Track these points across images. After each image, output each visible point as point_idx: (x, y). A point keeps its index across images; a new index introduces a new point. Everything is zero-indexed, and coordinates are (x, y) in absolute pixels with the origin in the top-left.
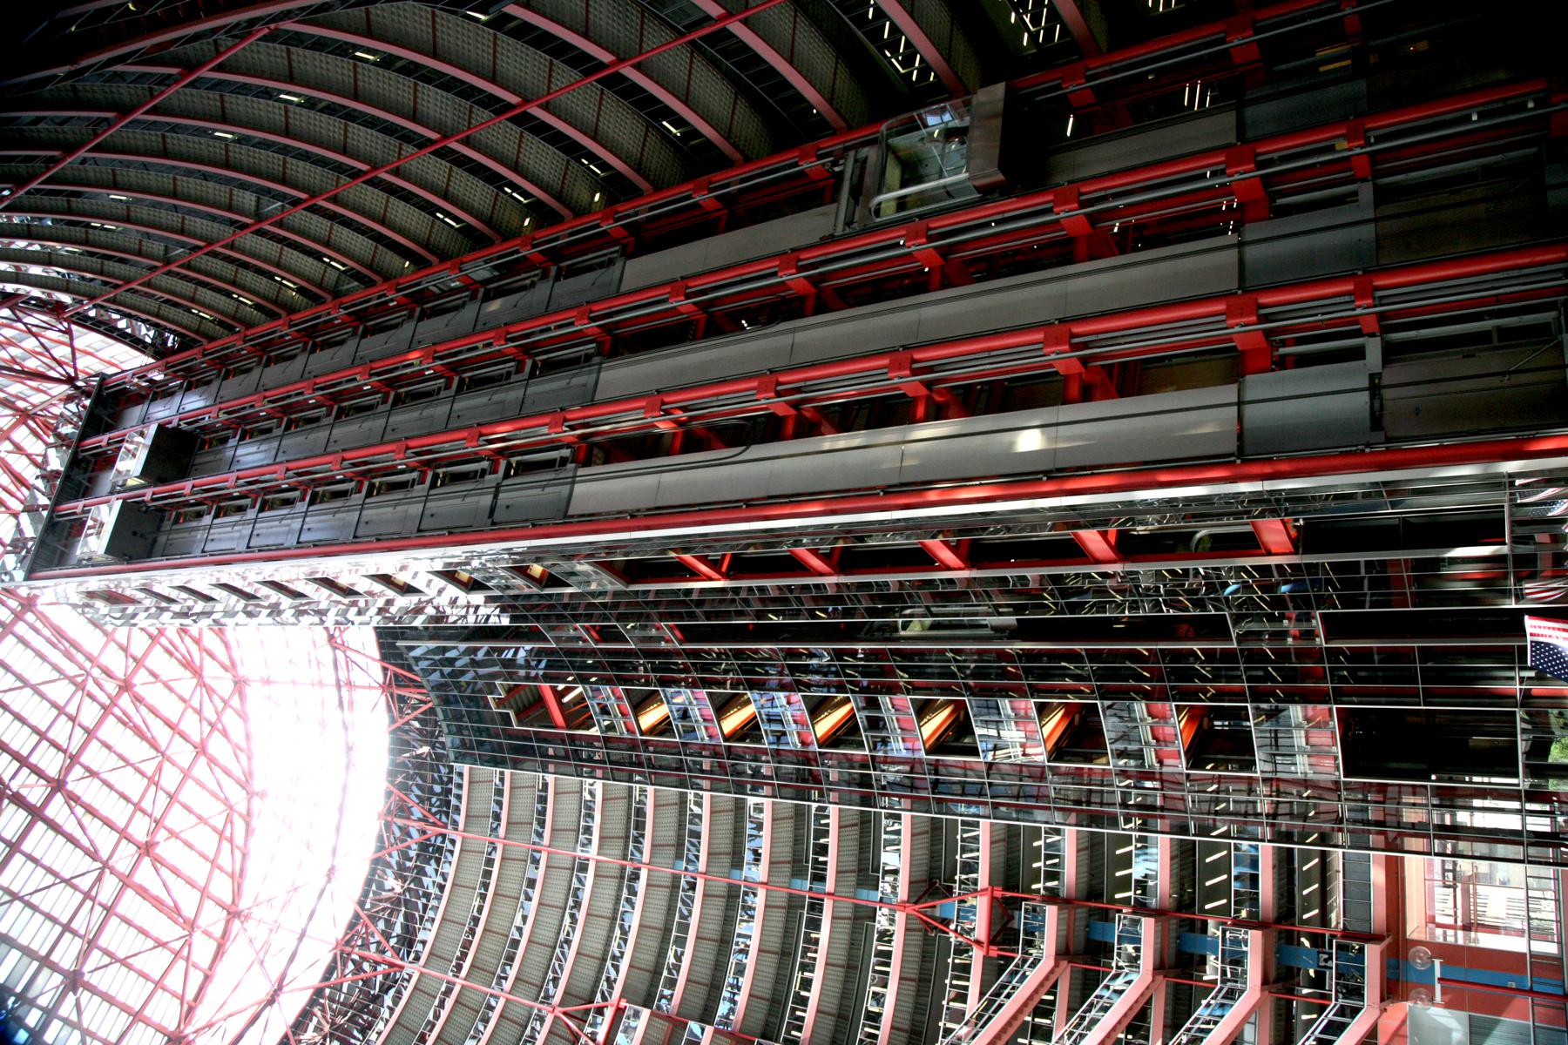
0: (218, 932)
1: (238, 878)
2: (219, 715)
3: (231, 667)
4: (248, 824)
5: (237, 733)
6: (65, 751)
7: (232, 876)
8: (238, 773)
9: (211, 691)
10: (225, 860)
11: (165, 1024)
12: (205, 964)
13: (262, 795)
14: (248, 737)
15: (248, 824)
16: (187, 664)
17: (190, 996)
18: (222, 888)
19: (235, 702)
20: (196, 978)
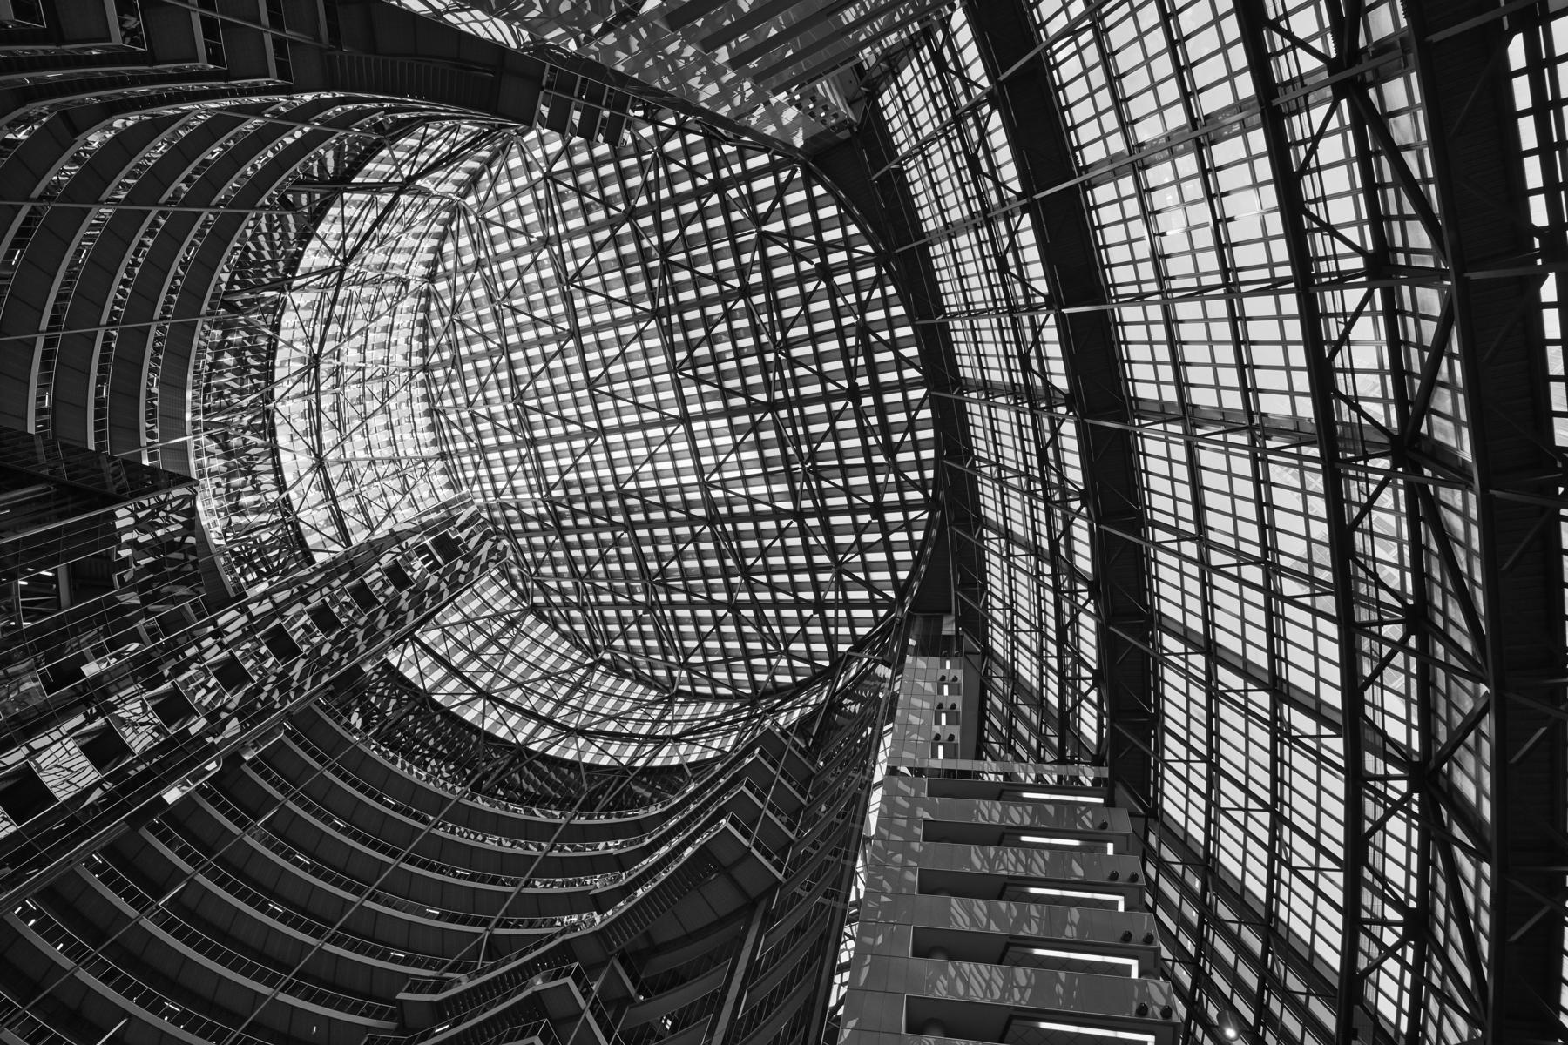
8: (462, 224)
9: (453, 289)
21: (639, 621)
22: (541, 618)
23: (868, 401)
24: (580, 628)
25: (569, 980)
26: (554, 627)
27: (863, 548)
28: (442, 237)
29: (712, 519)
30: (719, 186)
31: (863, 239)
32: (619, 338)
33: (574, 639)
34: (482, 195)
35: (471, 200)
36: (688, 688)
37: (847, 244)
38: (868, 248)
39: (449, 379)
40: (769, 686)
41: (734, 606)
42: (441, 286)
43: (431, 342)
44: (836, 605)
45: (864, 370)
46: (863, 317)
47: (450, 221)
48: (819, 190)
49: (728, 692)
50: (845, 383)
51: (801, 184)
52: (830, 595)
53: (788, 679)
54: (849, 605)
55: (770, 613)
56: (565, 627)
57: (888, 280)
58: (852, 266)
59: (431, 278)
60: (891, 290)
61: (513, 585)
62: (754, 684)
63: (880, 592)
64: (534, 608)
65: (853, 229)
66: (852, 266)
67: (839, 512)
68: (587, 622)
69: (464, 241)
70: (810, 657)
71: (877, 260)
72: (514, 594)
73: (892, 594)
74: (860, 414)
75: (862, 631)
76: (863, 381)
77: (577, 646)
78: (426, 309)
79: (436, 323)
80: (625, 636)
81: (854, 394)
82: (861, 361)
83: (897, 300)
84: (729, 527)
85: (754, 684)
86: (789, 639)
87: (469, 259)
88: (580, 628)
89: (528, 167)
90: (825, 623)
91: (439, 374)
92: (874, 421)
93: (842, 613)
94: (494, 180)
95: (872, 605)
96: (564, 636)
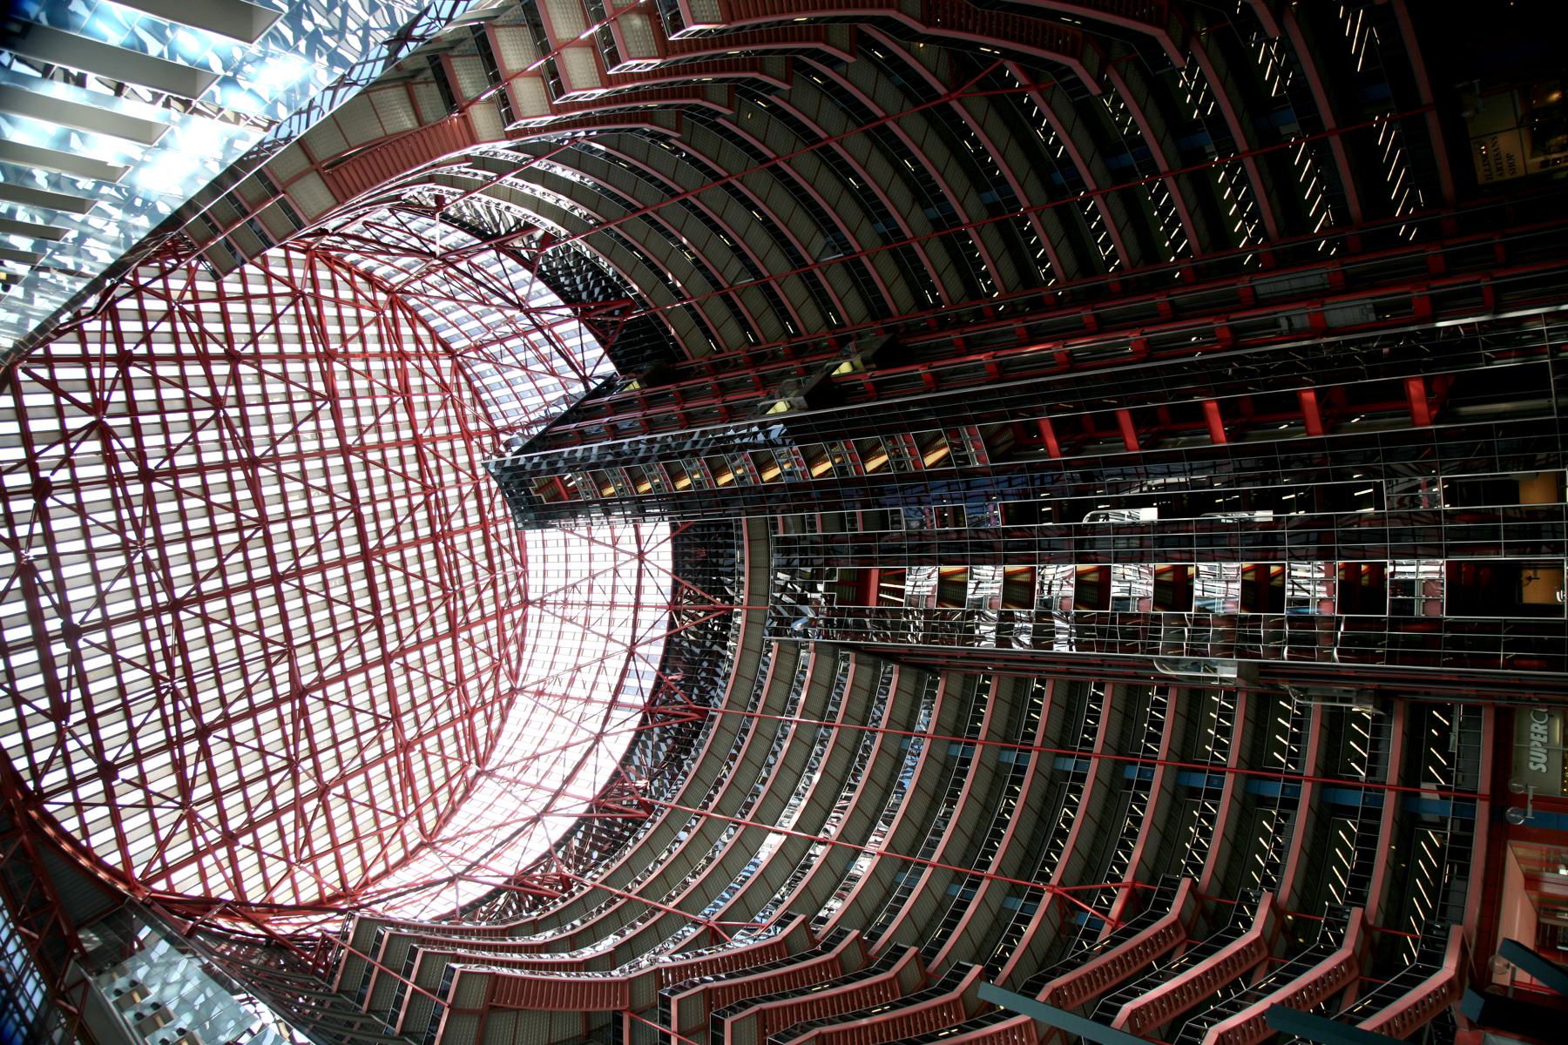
0: (411, 847)
1: (443, 820)
2: (492, 703)
3: (514, 676)
4: (467, 790)
5: (495, 724)
6: (401, 642)
7: (439, 817)
10: (443, 797)
11: (349, 877)
12: (392, 860)
13: (491, 774)
14: (499, 731)
15: (467, 790)
17: (372, 873)
18: (429, 817)
19: (504, 702)
20: (380, 867)
21: (344, 339)
23: (54, 625)
25: (674, 999)
26: (433, 333)
27: (64, 436)
29: (253, 463)
31: (58, 816)
33: (415, 319)
36: (293, 254)
37: (79, 806)
38: (50, 808)
41: (233, 358)
45: (58, 662)
46: (58, 726)
48: (114, 859)
50: (81, 644)
51: (135, 861)
52: (111, 372)
54: (85, 360)
55: (188, 349)
56: (422, 331)
57: (26, 775)
58: (73, 783)
60: (21, 764)
63: (37, 379)
64: (451, 353)
65: (71, 825)
66: (73, 783)
67: (94, 483)
68: (398, 338)
69: (481, 733)
71: (41, 797)
72: (468, 371)
73: (22, 376)
74: (64, 609)
76: (59, 649)
77: (411, 310)
81: (71, 633)
82: (62, 673)
83: (11, 754)
84: (232, 455)
86: (169, 316)
87: (479, 717)
88: (406, 331)
90: (119, 337)
92: (44, 601)
93: (94, 349)
95: (50, 361)
96: (424, 323)
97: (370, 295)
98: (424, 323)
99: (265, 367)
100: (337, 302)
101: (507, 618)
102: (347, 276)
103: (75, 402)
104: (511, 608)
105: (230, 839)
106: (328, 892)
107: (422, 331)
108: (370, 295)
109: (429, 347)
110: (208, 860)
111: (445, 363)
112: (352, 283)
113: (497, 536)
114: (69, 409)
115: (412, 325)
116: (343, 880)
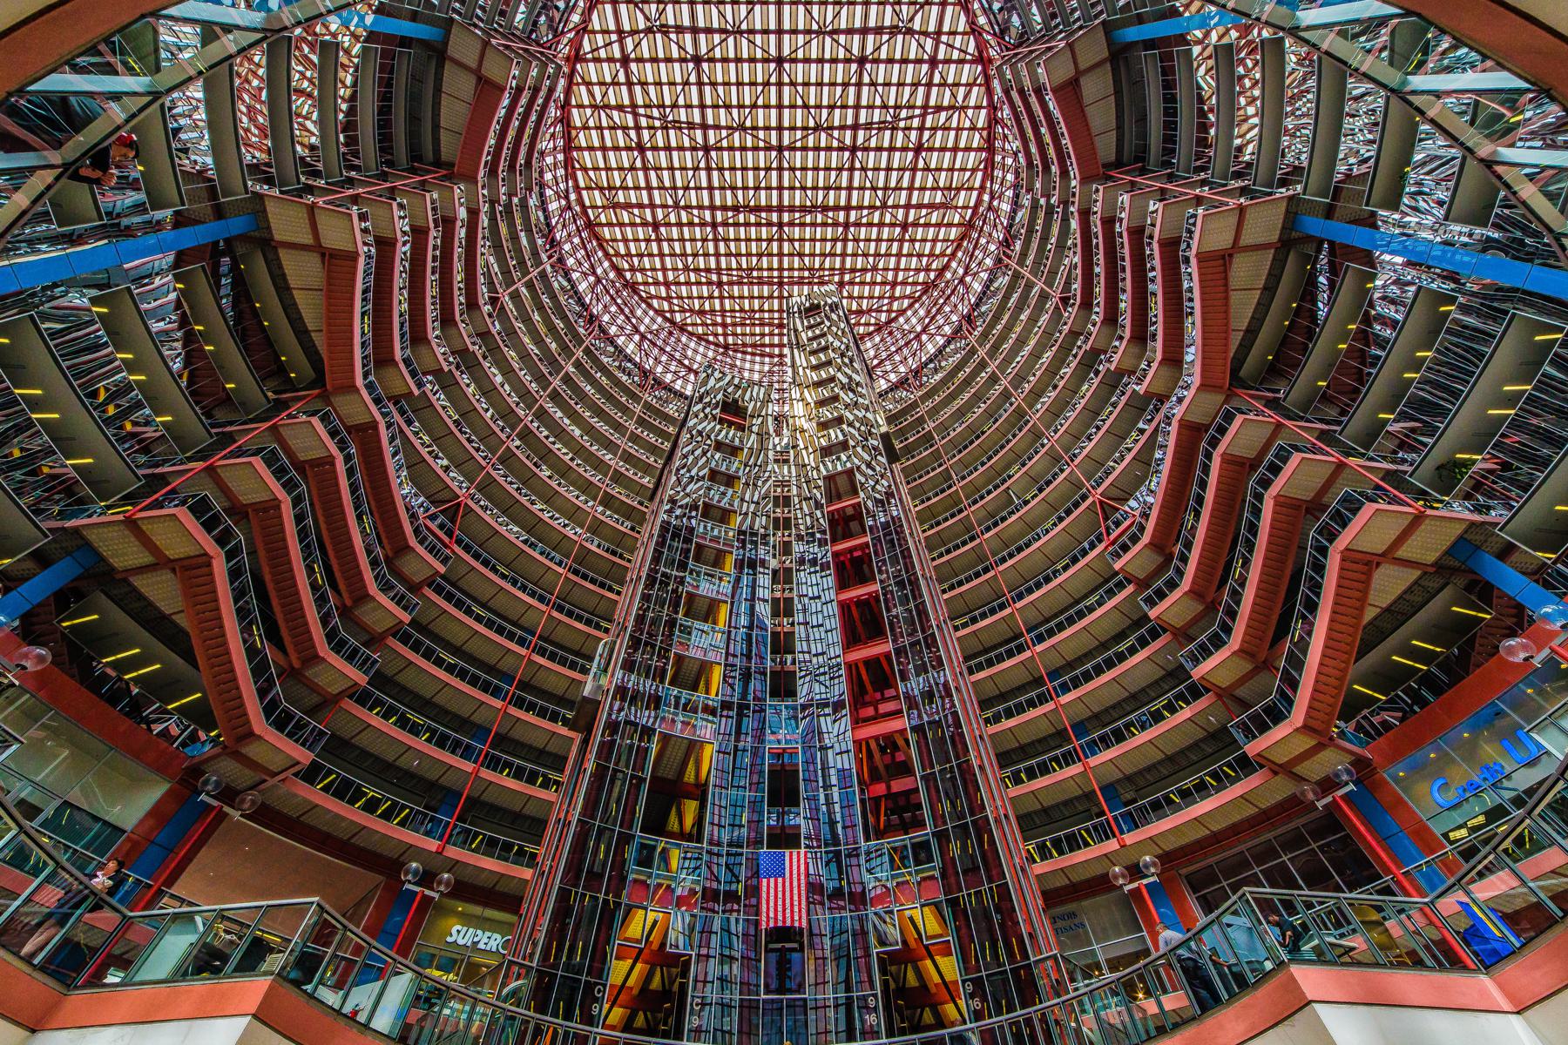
9: (683, 311)
16: (702, 312)
21: (912, 241)
22: (896, 319)
24: (908, 290)
28: (650, 306)
30: (625, 61)
32: (722, 188)
34: (626, 266)
35: (628, 275)
39: (735, 334)
40: (985, 133)
42: (678, 317)
43: (711, 338)
44: (937, 42)
47: (641, 297)
49: (980, 174)
53: (984, 112)
59: (672, 322)
61: (870, 334)
62: (979, 149)
69: (652, 290)
70: (970, 85)
75: (962, 25)
78: (692, 334)
79: (700, 330)
80: (920, 256)
85: (979, 149)
88: (908, 290)
89: (610, 225)
90: (948, 61)
91: (730, 340)
94: (617, 254)
96: (911, 306)
97: (934, 266)
98: (911, 306)
99: (907, 174)
100: (935, 241)
101: (720, 330)
102: (949, 251)
103: (916, 12)
104: (725, 335)
105: (625, 61)
106: (574, 133)
107: (906, 303)
108: (934, 266)
109: (895, 306)
110: (614, 37)
111: (883, 317)
112: (943, 254)
113: (771, 334)
114: (912, 8)
115: (909, 297)
116: (580, 149)
